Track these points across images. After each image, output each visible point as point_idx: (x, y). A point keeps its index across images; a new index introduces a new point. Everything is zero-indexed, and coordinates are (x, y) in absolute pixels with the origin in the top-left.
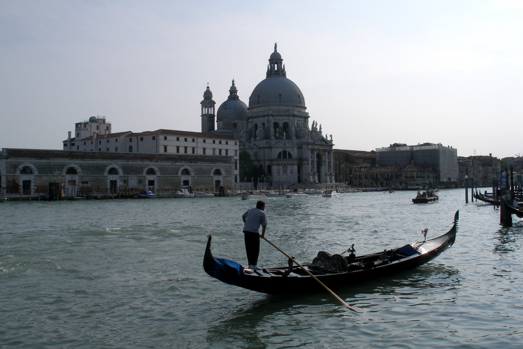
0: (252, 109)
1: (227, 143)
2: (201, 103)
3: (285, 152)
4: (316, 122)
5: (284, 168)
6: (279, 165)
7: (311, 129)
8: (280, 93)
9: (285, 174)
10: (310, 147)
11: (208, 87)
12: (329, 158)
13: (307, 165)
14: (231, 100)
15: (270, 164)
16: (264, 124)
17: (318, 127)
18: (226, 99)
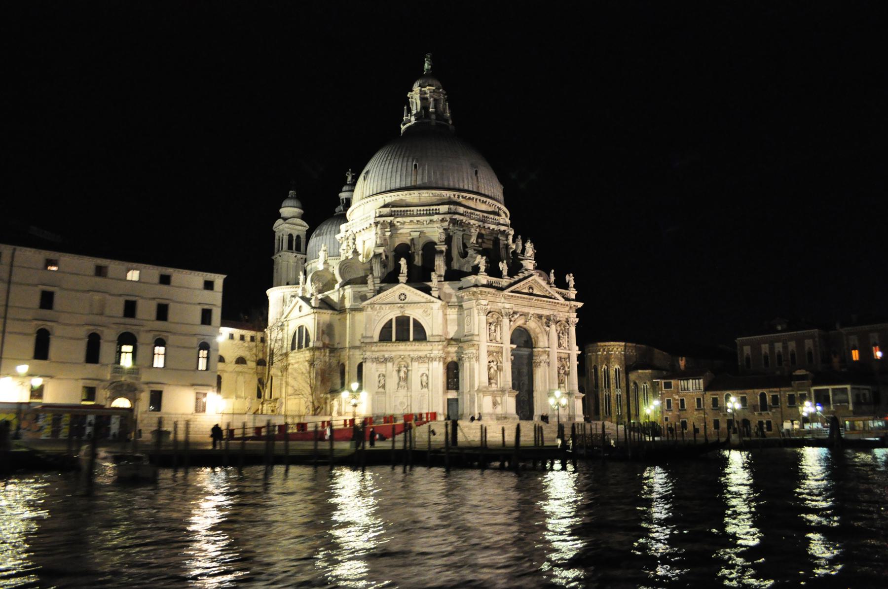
3: (403, 322)
5: (399, 371)
6: (386, 360)
9: (402, 392)
12: (565, 344)
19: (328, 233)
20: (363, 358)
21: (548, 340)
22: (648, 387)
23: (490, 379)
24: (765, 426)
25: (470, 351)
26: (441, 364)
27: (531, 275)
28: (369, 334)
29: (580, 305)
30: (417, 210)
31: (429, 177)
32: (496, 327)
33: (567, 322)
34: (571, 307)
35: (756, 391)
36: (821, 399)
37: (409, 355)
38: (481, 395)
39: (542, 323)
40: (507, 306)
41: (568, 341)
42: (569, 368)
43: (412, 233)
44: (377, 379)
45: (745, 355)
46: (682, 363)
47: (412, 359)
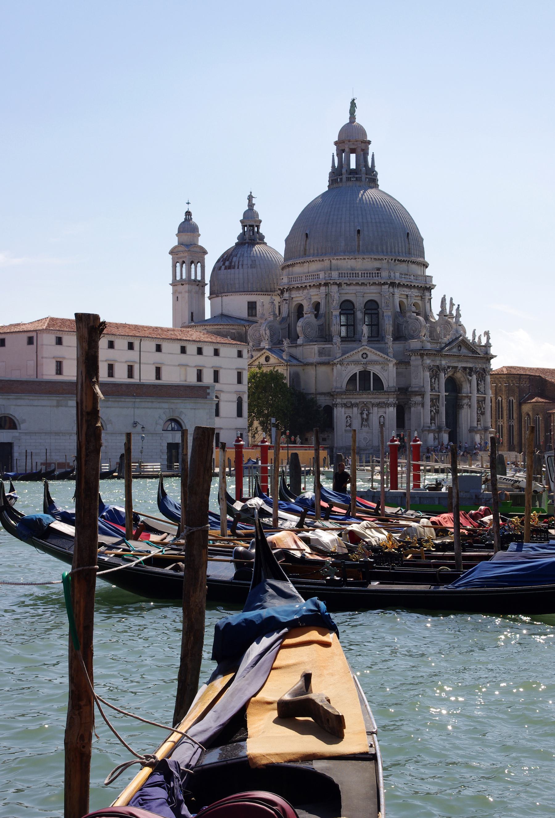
0: (291, 269)
1: (216, 353)
2: (171, 253)
3: (365, 375)
4: (451, 299)
5: (362, 414)
6: (352, 405)
7: (437, 318)
8: (359, 228)
10: (428, 361)
11: (188, 213)
13: (420, 407)
14: (245, 244)
15: (331, 405)
16: (317, 306)
17: (454, 312)
18: (232, 241)
19: (240, 267)
20: (333, 405)
21: (470, 387)
22: (540, 418)
23: (431, 420)
26: (395, 408)
28: (339, 385)
30: (362, 273)
32: (435, 379)
39: (466, 375)
40: (443, 362)
41: (484, 387)
42: (484, 409)
44: (344, 420)
47: (373, 405)
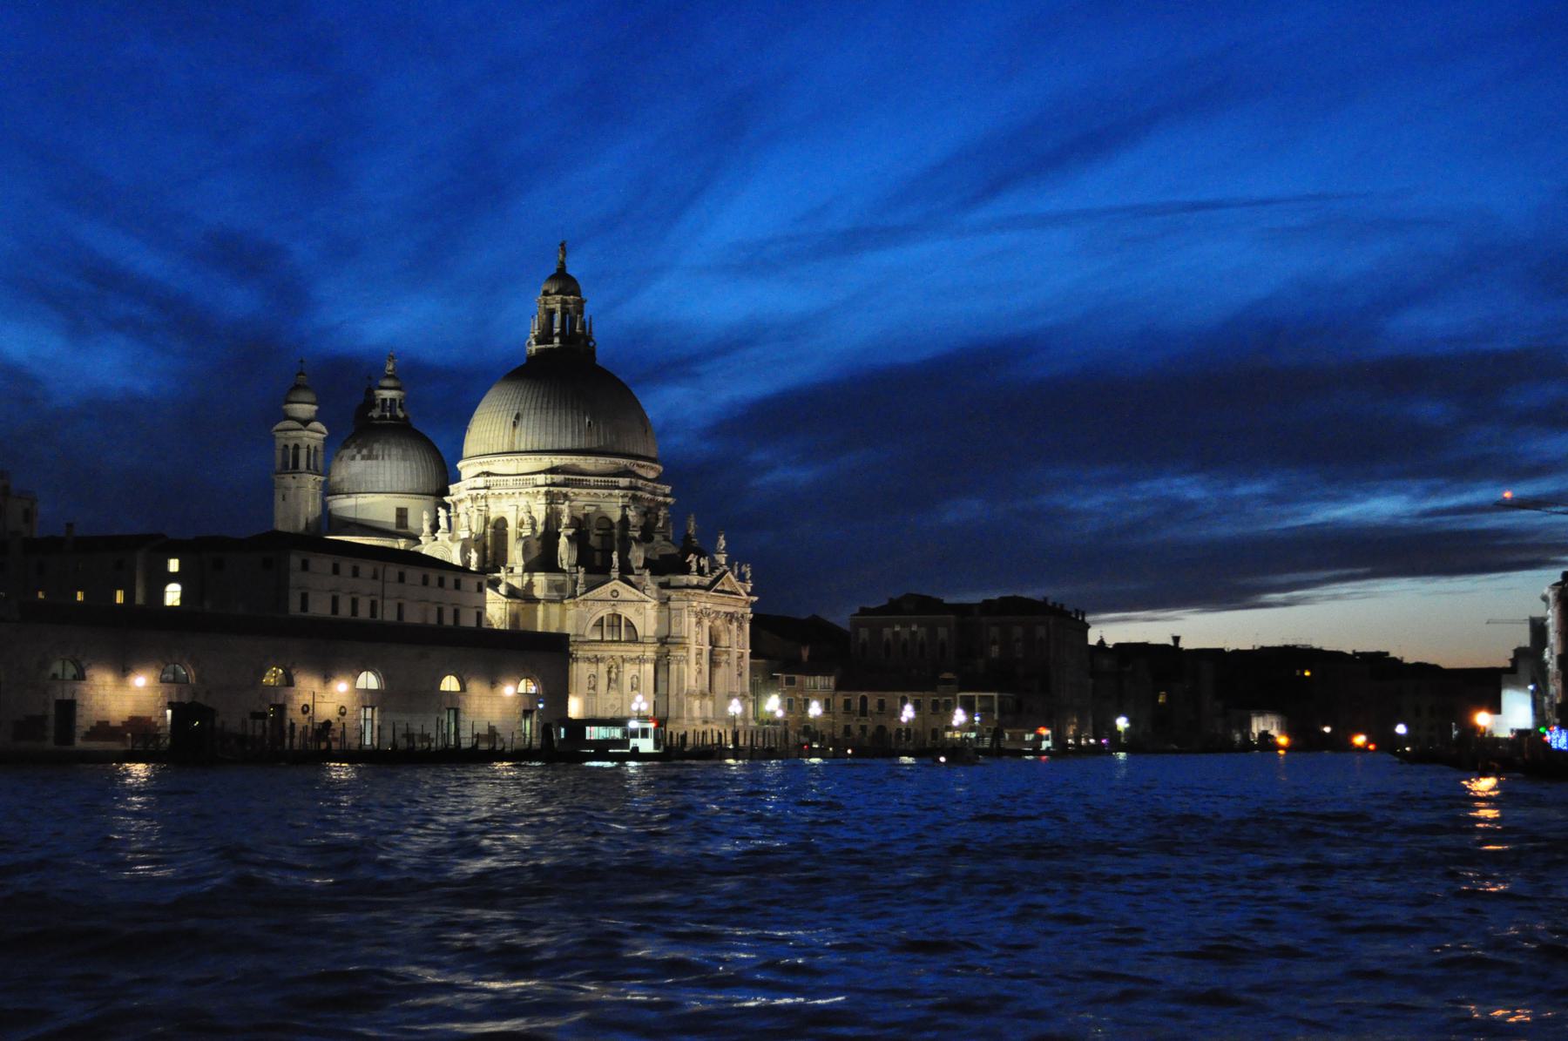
6: (598, 660)
9: (613, 694)
19: (386, 457)
21: (730, 639)
22: (760, 681)
24: (904, 734)
25: (677, 653)
27: (725, 572)
29: (755, 599)
31: (605, 439)
33: (742, 616)
34: (747, 603)
35: (896, 693)
36: (969, 708)
37: (622, 656)
38: (692, 699)
40: (708, 606)
43: (587, 508)
44: (587, 681)
45: (860, 641)
46: (805, 653)
